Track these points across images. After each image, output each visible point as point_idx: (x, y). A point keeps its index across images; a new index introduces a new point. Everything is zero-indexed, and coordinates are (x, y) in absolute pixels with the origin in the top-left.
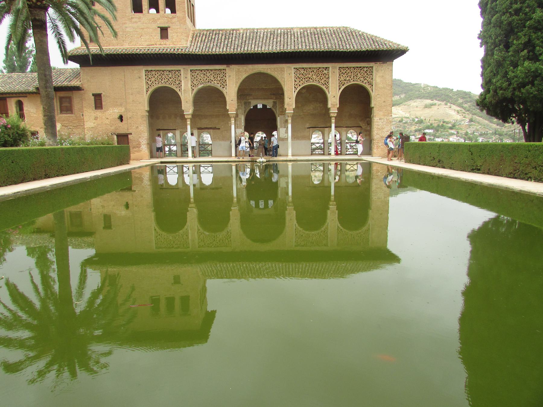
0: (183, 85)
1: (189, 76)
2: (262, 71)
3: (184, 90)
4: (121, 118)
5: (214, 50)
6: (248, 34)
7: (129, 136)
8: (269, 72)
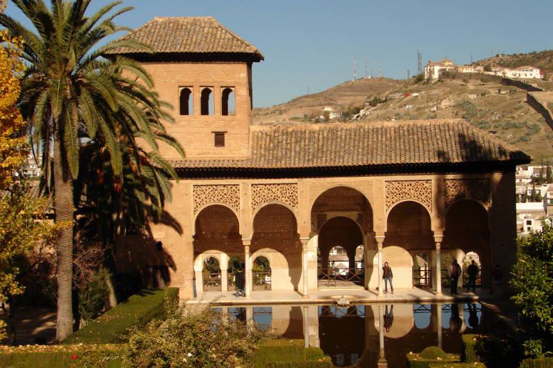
0: (241, 201)
1: (250, 192)
2: (345, 185)
3: (243, 210)
5: (283, 162)
6: (325, 135)
8: (352, 186)
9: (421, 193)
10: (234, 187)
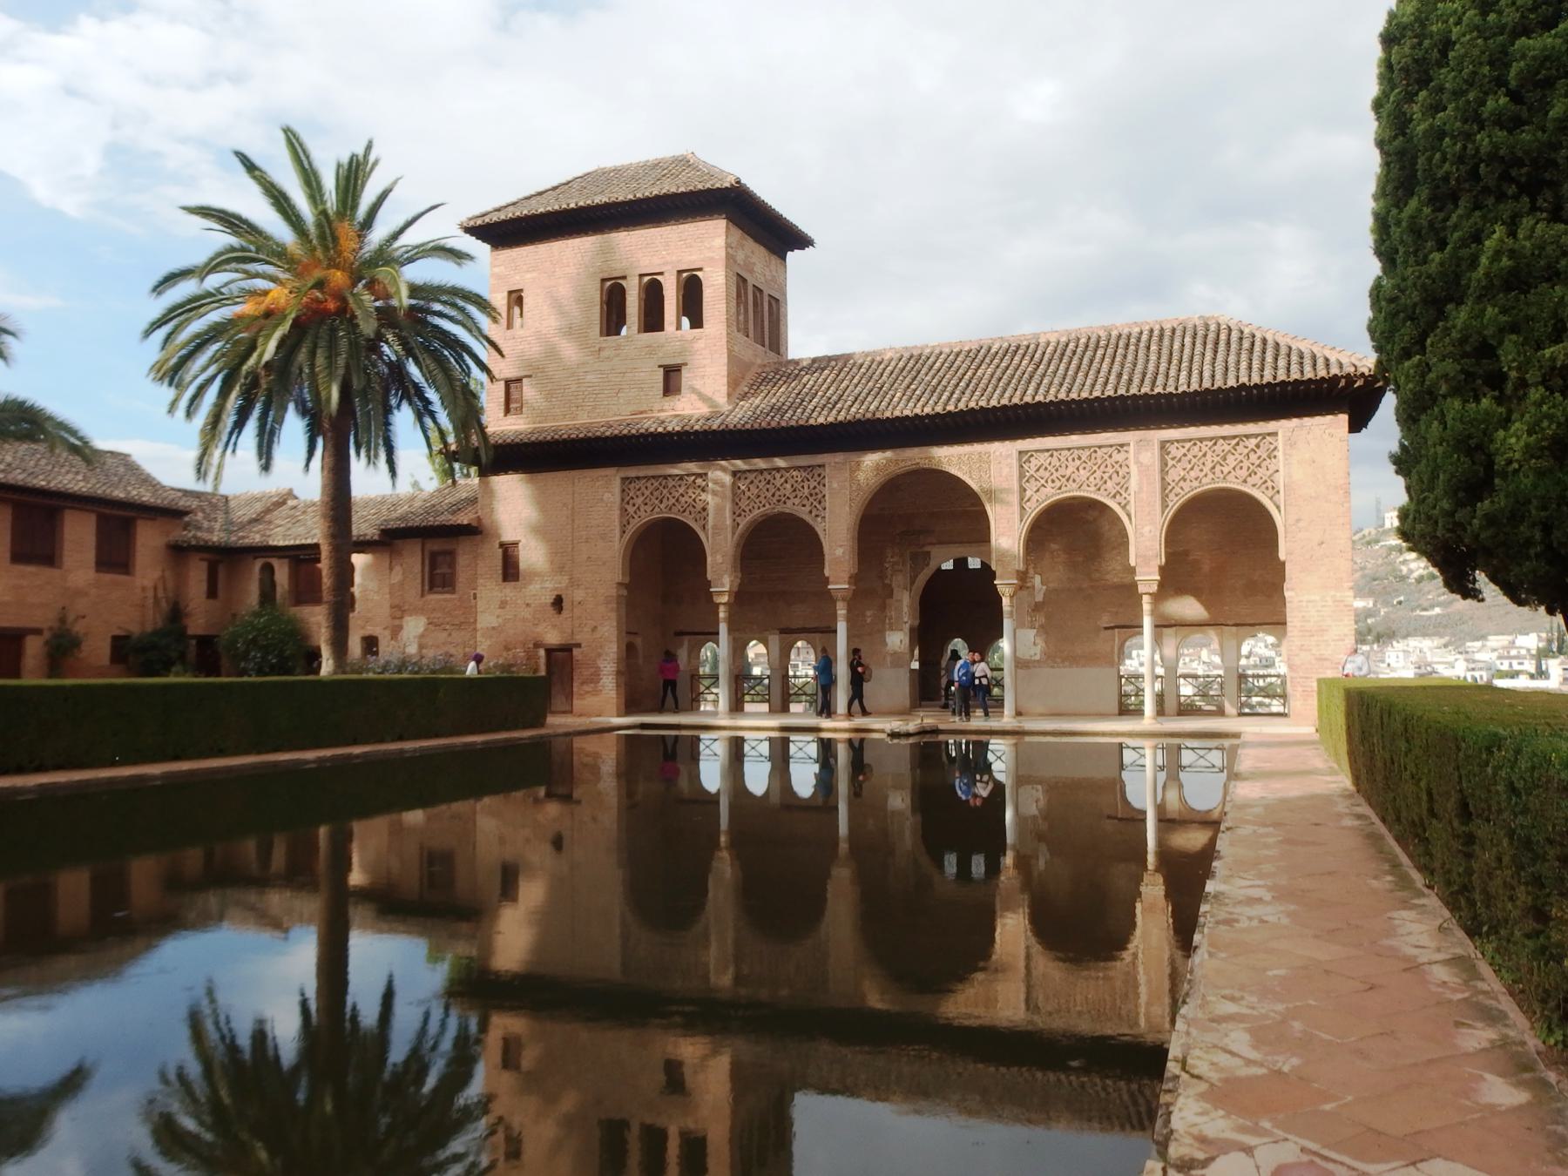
3: (715, 527)
4: (558, 603)
7: (576, 651)
9: (1106, 476)
10: (699, 481)
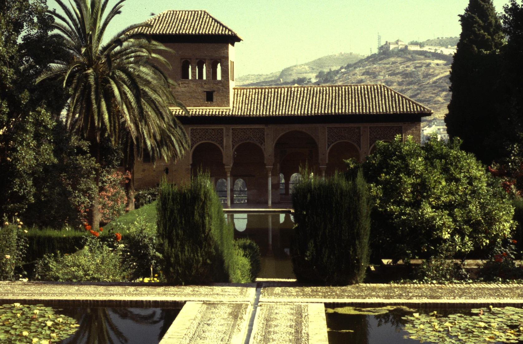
1: (231, 134)
3: (226, 146)
8: (304, 130)
